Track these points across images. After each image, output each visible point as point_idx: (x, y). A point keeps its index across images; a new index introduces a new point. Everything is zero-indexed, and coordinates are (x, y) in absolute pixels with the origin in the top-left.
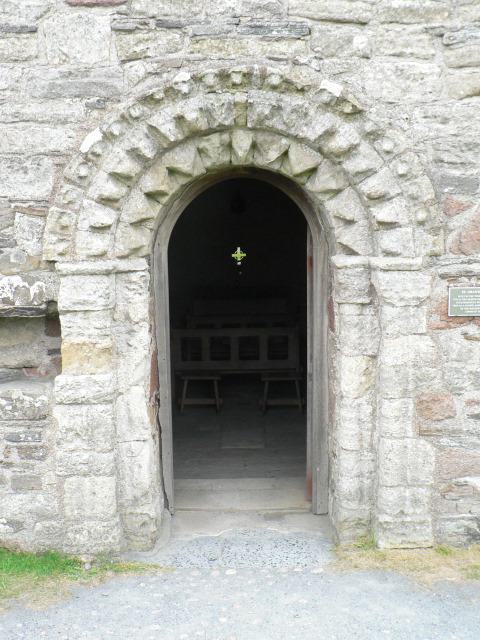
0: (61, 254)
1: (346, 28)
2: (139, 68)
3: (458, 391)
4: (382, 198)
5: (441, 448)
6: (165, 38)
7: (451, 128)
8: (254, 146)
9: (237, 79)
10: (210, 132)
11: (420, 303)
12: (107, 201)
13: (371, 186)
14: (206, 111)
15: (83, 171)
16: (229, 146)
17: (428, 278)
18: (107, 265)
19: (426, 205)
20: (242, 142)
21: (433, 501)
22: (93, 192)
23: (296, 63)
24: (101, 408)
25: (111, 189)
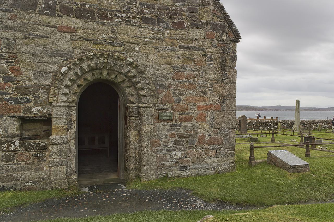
0: (54, 101)
1: (133, 45)
2: (78, 51)
3: (161, 139)
4: (142, 89)
5: (157, 154)
6: (86, 43)
7: (159, 72)
8: (108, 74)
9: (106, 56)
10: (96, 69)
11: (152, 116)
12: (67, 86)
13: (139, 85)
14: (96, 64)
15: (62, 78)
16: (101, 74)
17: (153, 110)
18: (67, 104)
19: (154, 91)
20: (105, 73)
21: (155, 169)
22: (64, 84)
23: (121, 53)
24: (64, 145)
25: (69, 83)
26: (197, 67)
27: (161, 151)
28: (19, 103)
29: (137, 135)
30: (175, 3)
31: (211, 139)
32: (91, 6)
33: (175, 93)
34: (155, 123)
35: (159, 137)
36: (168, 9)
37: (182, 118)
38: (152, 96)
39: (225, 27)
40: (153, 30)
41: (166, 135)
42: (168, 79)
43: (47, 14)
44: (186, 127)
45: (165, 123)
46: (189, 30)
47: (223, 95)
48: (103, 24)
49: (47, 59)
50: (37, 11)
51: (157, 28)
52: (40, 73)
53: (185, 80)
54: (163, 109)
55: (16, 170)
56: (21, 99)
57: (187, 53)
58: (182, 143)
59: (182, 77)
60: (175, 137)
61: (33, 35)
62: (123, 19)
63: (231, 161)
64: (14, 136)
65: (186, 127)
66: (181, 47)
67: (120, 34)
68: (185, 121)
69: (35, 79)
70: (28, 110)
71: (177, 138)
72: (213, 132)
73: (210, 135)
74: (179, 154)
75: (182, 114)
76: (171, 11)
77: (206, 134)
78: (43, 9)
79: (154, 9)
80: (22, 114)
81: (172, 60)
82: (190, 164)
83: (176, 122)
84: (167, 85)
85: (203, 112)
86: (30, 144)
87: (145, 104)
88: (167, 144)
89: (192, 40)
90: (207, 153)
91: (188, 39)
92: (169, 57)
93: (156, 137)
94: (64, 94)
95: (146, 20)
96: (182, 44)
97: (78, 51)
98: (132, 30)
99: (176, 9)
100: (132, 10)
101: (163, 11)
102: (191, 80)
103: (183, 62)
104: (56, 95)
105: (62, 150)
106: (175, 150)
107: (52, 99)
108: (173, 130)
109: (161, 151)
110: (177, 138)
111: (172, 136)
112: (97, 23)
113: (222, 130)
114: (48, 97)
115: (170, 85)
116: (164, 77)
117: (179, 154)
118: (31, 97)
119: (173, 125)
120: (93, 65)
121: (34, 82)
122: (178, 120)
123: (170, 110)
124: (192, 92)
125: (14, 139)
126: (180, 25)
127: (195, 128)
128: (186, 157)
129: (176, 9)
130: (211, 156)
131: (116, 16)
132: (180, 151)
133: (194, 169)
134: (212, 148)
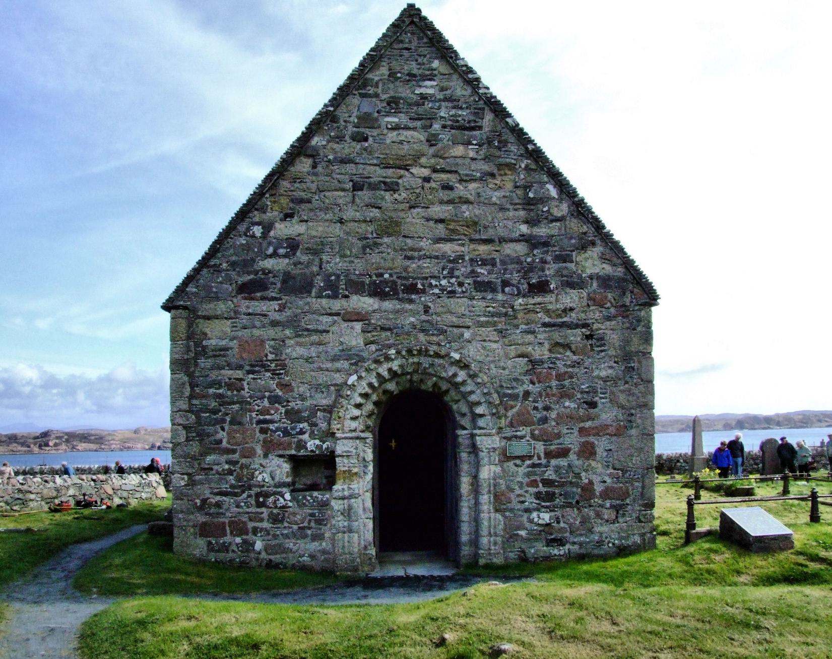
11: (494, 449)
19: (496, 406)
26: (575, 358)
31: (607, 488)
33: (536, 408)
35: (508, 487)
37: (551, 452)
38: (494, 414)
41: (521, 483)
42: (523, 383)
44: (557, 469)
45: (518, 462)
46: (557, 295)
54: (516, 437)
57: (557, 336)
58: (550, 497)
59: (548, 377)
60: (537, 486)
65: (557, 469)
66: (545, 325)
72: (610, 475)
73: (605, 482)
75: (551, 445)
77: (596, 479)
81: (530, 348)
83: (539, 458)
84: (521, 395)
85: (591, 439)
87: (483, 428)
88: (522, 499)
91: (558, 310)
96: (547, 320)
99: (533, 261)
102: (567, 383)
106: (538, 510)
108: (534, 474)
111: (533, 483)
113: (627, 471)
115: (527, 394)
116: (516, 380)
119: (534, 466)
123: (528, 438)
124: (567, 404)
126: (542, 288)
128: (558, 522)
130: (607, 521)
132: (547, 512)
133: (574, 543)
134: (608, 505)
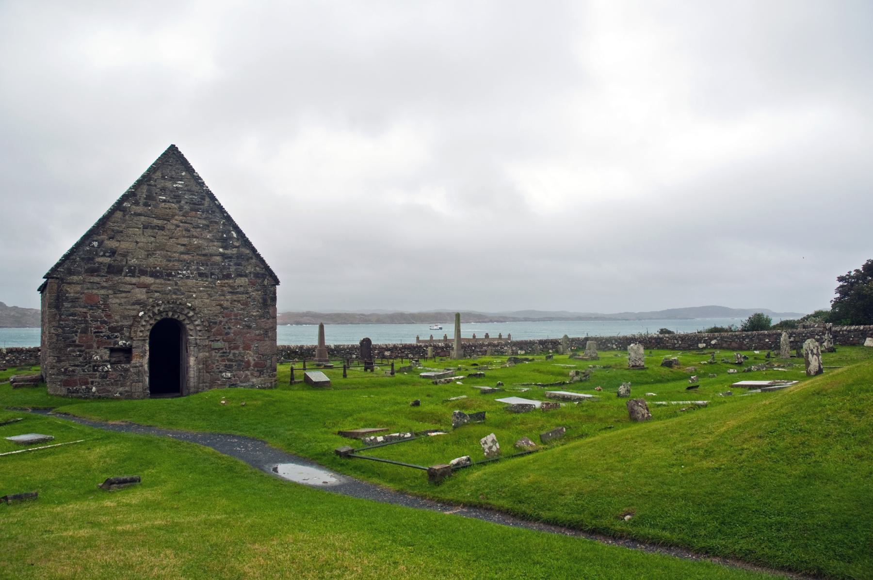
2: (151, 300)
3: (214, 363)
5: (211, 375)
11: (206, 346)
13: (197, 323)
16: (167, 315)
18: (143, 338)
20: (170, 314)
22: (141, 324)
25: (144, 323)
26: (242, 307)
27: (213, 372)
28: (111, 338)
29: (195, 361)
30: (224, 260)
32: (160, 268)
33: (224, 328)
34: (208, 352)
36: (218, 265)
39: (266, 275)
40: (206, 281)
43: (130, 276)
45: (216, 351)
47: (266, 328)
48: (169, 280)
49: (128, 307)
50: (123, 274)
51: (209, 279)
52: (125, 317)
53: (233, 317)
55: (109, 385)
56: (112, 336)
57: (235, 297)
61: (120, 291)
62: (184, 275)
63: (273, 381)
64: (107, 361)
66: (230, 292)
67: (182, 286)
68: (233, 349)
69: (121, 321)
70: (116, 343)
71: (227, 363)
72: (257, 357)
74: (229, 375)
76: (221, 266)
78: (127, 273)
79: (207, 266)
80: (112, 346)
82: (239, 382)
83: (226, 350)
86: (117, 367)
89: (238, 286)
90: (252, 374)
92: (219, 300)
93: (210, 362)
94: (141, 331)
95: (201, 275)
97: (151, 300)
98: (190, 282)
99: (225, 265)
100: (190, 268)
101: (215, 267)
103: (231, 303)
104: (135, 332)
105: (139, 371)
106: (226, 372)
107: (133, 335)
108: (223, 356)
109: (213, 372)
110: (227, 363)
111: (223, 361)
112: (165, 279)
114: (130, 333)
115: (221, 322)
117: (229, 375)
118: (118, 334)
119: (224, 353)
120: (161, 309)
121: (120, 324)
122: (227, 348)
125: (107, 364)
126: (228, 276)
127: (242, 355)
129: (225, 265)
131: (178, 273)
